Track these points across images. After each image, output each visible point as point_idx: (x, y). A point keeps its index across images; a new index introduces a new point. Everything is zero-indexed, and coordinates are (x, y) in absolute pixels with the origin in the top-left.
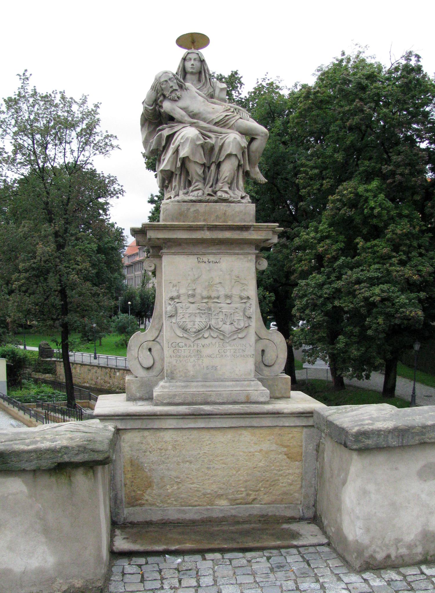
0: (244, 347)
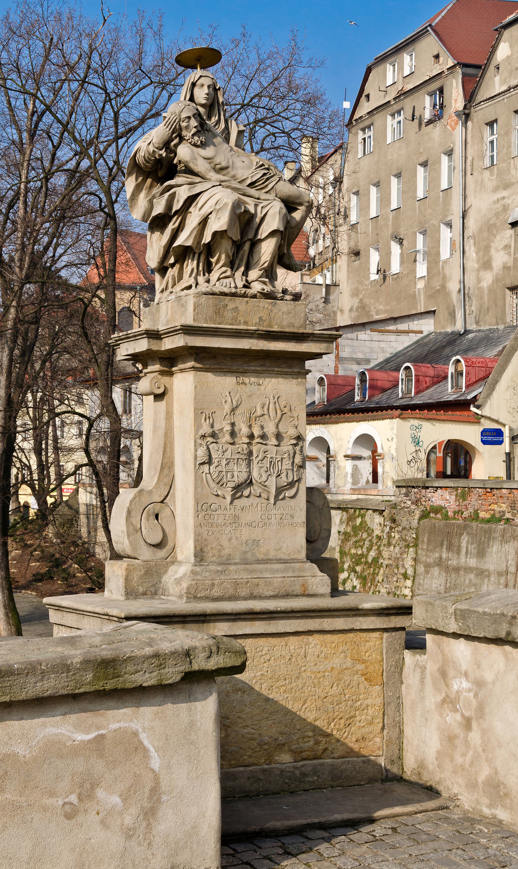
0: (292, 511)
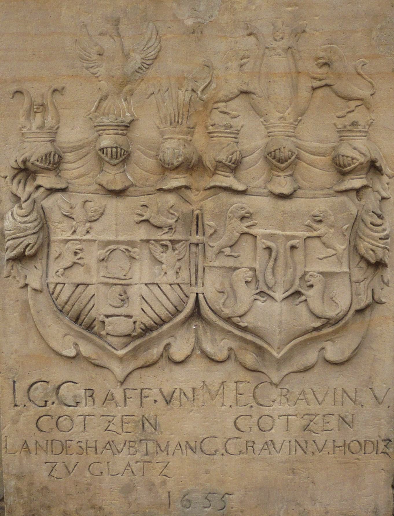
0: (349, 404)
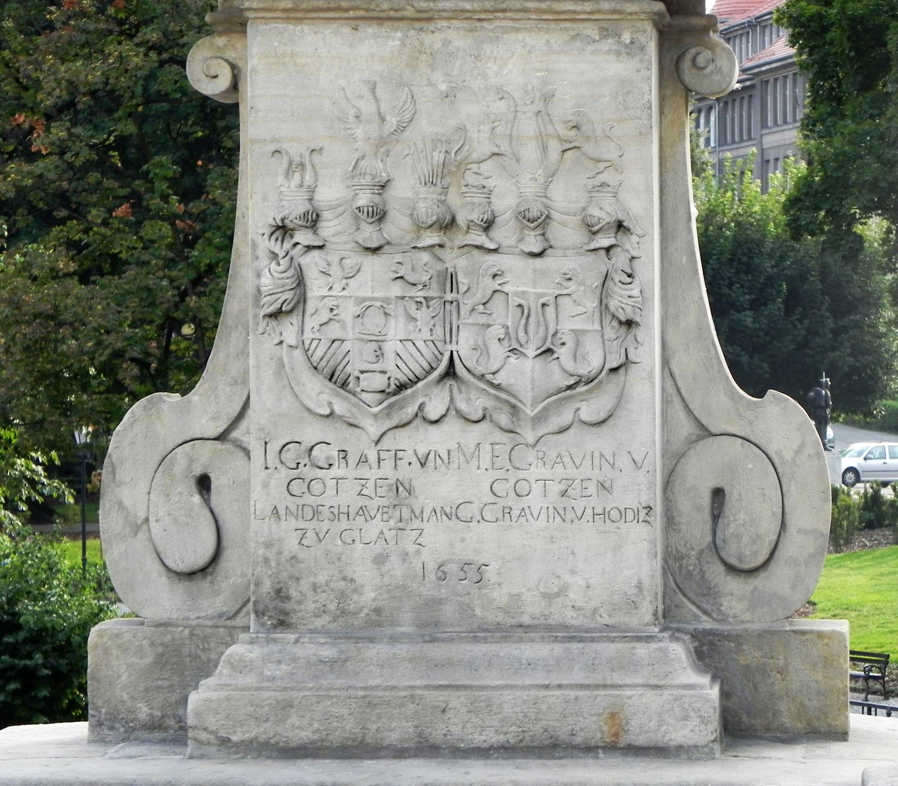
0: (606, 467)
